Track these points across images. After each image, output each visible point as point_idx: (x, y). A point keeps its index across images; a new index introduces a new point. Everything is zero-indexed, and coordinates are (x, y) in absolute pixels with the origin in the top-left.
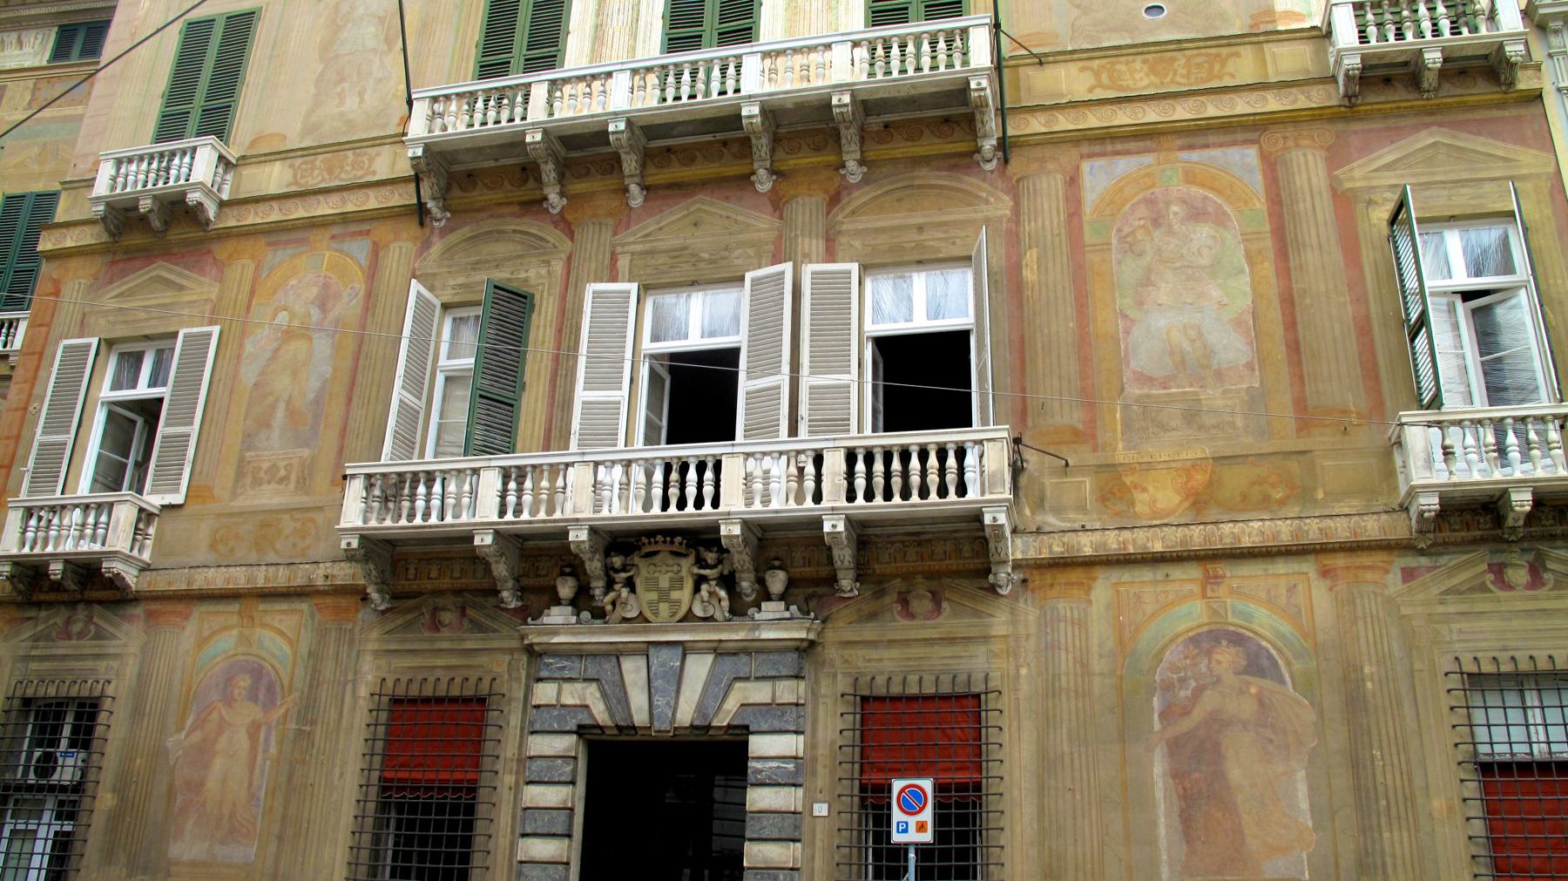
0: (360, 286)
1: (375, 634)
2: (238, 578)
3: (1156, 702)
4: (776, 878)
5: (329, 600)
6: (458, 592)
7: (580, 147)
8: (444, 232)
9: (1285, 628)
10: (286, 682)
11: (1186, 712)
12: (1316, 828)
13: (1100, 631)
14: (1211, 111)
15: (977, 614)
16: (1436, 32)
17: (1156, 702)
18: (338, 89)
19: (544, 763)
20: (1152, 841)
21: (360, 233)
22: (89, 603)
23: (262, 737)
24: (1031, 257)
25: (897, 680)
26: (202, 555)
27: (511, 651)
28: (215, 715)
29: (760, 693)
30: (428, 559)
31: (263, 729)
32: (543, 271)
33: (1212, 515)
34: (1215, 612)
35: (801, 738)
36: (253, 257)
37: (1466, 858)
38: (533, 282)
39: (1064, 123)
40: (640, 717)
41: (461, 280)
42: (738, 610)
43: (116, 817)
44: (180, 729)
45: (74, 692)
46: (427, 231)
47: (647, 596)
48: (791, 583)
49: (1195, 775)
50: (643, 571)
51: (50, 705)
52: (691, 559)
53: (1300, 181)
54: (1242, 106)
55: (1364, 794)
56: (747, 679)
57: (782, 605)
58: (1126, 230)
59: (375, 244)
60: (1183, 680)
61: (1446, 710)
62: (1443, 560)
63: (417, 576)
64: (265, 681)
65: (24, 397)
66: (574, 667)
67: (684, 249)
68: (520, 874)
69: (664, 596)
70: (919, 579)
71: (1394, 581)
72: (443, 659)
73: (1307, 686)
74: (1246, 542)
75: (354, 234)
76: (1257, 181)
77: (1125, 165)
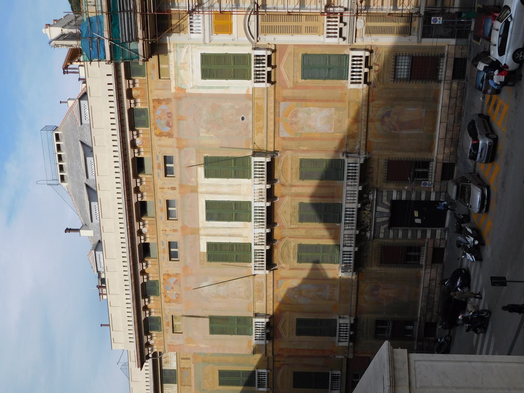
0: (291, 280)
16: (264, 67)
24: (302, 148)
29: (385, 198)
40: (387, 219)
41: (292, 259)
54: (271, 104)
74: (366, 115)
76: (289, 103)
77: (282, 128)
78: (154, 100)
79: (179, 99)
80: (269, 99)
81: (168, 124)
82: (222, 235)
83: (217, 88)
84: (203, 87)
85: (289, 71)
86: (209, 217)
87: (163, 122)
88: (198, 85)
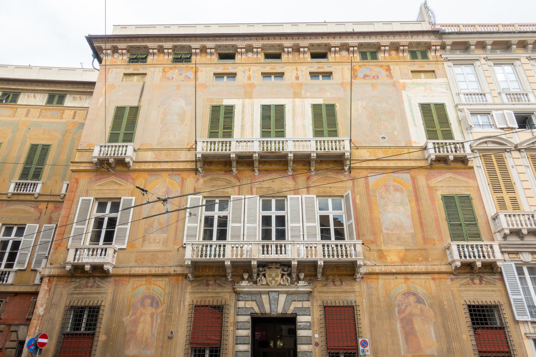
1: (189, 287)
2: (146, 270)
3: (396, 309)
4: (307, 354)
5: (174, 278)
6: (214, 276)
7: (242, 159)
8: (203, 177)
9: (425, 292)
10: (162, 301)
11: (404, 312)
12: (437, 342)
13: (381, 291)
14: (399, 165)
15: (352, 285)
17: (396, 309)
18: (167, 133)
19: (242, 324)
20: (398, 345)
21: (178, 174)
22: (94, 277)
23: (155, 317)
24: (358, 197)
25: (333, 302)
26: (132, 264)
27: (230, 292)
28: (139, 311)
29: (299, 305)
30: (205, 267)
31: (155, 315)
32: (232, 190)
33: (406, 263)
34: (408, 287)
35: (310, 317)
36: (144, 178)
37: (472, 350)
38: (230, 192)
39: (364, 164)
40: (268, 311)
42: (292, 283)
43: (106, 343)
44: (128, 315)
45: (87, 304)
46: (198, 176)
47: (269, 279)
48: (305, 276)
49: (407, 328)
50: (268, 272)
51: (79, 308)
52: (281, 269)
53: (420, 183)
54: (406, 164)
55: (448, 334)
56: (295, 301)
57: (304, 282)
58: (380, 192)
59: (182, 178)
60: (402, 304)
61: (464, 313)
62: (460, 277)
63: (205, 272)
64: (155, 301)
65: (67, 213)
66: (249, 297)
67: (270, 187)
68: (236, 355)
69: (274, 279)
70: (336, 276)
71: (449, 282)
72: (211, 295)
73: (431, 306)
74: (415, 270)
75: (175, 174)
76: (410, 182)
78: (389, 66)
79: (394, 85)
80: (412, 162)
81: (365, 76)
82: (243, 119)
83: (413, 116)
84: (410, 105)
85: (447, 183)
86: (266, 109)
87: (368, 72)
88: (412, 101)
